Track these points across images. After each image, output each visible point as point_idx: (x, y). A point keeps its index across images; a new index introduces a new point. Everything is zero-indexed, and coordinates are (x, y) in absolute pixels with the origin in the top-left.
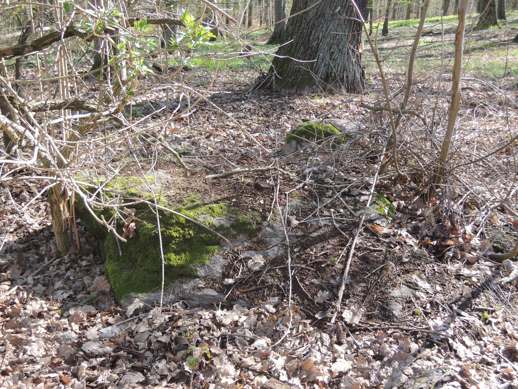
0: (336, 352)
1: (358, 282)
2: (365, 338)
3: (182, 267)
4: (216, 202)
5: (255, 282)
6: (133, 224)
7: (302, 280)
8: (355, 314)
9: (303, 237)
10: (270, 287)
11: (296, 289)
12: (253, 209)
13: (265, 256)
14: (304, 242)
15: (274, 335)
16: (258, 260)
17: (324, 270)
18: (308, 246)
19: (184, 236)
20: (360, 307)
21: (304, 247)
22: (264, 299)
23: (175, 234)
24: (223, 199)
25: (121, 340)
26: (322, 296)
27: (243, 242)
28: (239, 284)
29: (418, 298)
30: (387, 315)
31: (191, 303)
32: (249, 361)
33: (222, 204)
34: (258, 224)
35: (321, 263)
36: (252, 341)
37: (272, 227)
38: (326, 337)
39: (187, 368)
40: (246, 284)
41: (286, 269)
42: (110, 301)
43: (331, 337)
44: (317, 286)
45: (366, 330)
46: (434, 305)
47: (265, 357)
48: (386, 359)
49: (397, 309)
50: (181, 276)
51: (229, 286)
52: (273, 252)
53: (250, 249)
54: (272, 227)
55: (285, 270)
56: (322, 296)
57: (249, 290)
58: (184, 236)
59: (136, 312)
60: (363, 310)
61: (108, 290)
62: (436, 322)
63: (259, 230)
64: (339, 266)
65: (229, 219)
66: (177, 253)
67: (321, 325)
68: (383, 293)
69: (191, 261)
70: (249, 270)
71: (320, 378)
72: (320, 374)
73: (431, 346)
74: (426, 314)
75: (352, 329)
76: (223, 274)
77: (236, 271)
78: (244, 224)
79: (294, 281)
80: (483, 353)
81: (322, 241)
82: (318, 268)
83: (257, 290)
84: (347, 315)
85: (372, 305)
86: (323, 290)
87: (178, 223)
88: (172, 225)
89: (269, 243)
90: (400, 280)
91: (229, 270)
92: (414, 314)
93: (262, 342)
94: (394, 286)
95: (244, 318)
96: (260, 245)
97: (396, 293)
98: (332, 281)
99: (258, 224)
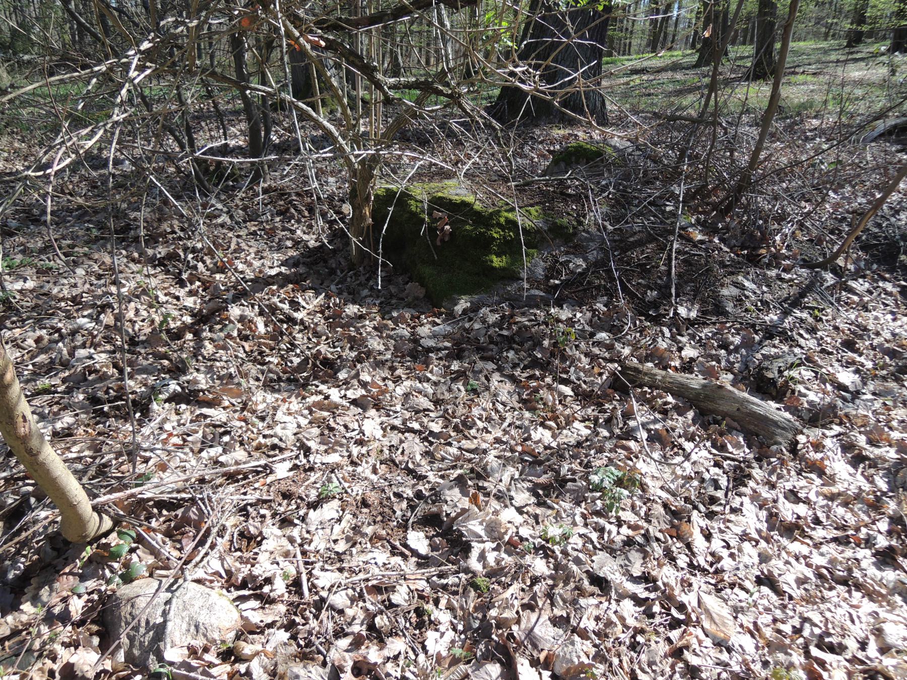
0: (680, 342)
1: (686, 283)
2: (706, 330)
3: (503, 269)
4: (532, 205)
5: (582, 284)
6: (447, 227)
7: (629, 281)
8: (689, 310)
9: (621, 241)
10: (598, 288)
11: (625, 289)
12: (568, 214)
13: (585, 260)
14: (623, 244)
15: (615, 330)
16: (579, 264)
17: (649, 271)
18: (628, 250)
19: (504, 238)
20: (693, 304)
21: (624, 250)
22: (594, 298)
23: (495, 235)
24: (537, 204)
25: (458, 336)
26: (652, 294)
27: (559, 247)
28: (566, 284)
29: (747, 297)
30: (719, 310)
31: (516, 302)
32: (596, 350)
33: (537, 207)
34: (574, 228)
35: (646, 265)
36: (592, 335)
37: (588, 232)
38: (666, 330)
39: (539, 356)
40: (573, 283)
41: (610, 271)
42: (434, 302)
43: (670, 331)
44: (644, 286)
45: (704, 324)
46: (765, 303)
47: (610, 348)
48: (732, 347)
49: (730, 308)
50: (503, 278)
51: (556, 287)
52: (593, 256)
53: (567, 253)
54: (588, 232)
55: (609, 271)
56: (652, 294)
57: (577, 291)
58: (504, 238)
59: (465, 312)
60: (697, 306)
61: (422, 296)
62: (772, 317)
63: (575, 234)
64: (663, 268)
65: (546, 221)
66: (498, 255)
67: (657, 320)
68: (714, 292)
69: (512, 264)
70: (572, 272)
71: (673, 364)
72: (672, 360)
73: (771, 337)
74: (759, 310)
75: (690, 323)
76: (546, 276)
77: (559, 273)
78: (562, 227)
79: (621, 282)
80: (820, 345)
81: (640, 246)
82: (644, 269)
83: (585, 290)
84: (682, 311)
85: (703, 302)
86: (652, 290)
87: (499, 225)
88: (493, 226)
89: (587, 247)
90: (727, 280)
91: (552, 271)
92: (747, 310)
93: (603, 336)
94: (722, 285)
95: (579, 315)
96: (579, 250)
97: (725, 292)
98: (659, 281)
99: (574, 228)
